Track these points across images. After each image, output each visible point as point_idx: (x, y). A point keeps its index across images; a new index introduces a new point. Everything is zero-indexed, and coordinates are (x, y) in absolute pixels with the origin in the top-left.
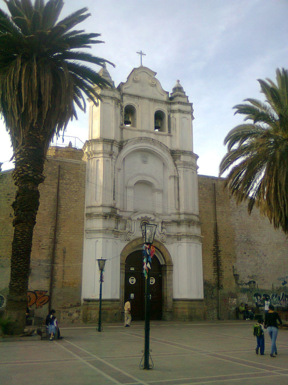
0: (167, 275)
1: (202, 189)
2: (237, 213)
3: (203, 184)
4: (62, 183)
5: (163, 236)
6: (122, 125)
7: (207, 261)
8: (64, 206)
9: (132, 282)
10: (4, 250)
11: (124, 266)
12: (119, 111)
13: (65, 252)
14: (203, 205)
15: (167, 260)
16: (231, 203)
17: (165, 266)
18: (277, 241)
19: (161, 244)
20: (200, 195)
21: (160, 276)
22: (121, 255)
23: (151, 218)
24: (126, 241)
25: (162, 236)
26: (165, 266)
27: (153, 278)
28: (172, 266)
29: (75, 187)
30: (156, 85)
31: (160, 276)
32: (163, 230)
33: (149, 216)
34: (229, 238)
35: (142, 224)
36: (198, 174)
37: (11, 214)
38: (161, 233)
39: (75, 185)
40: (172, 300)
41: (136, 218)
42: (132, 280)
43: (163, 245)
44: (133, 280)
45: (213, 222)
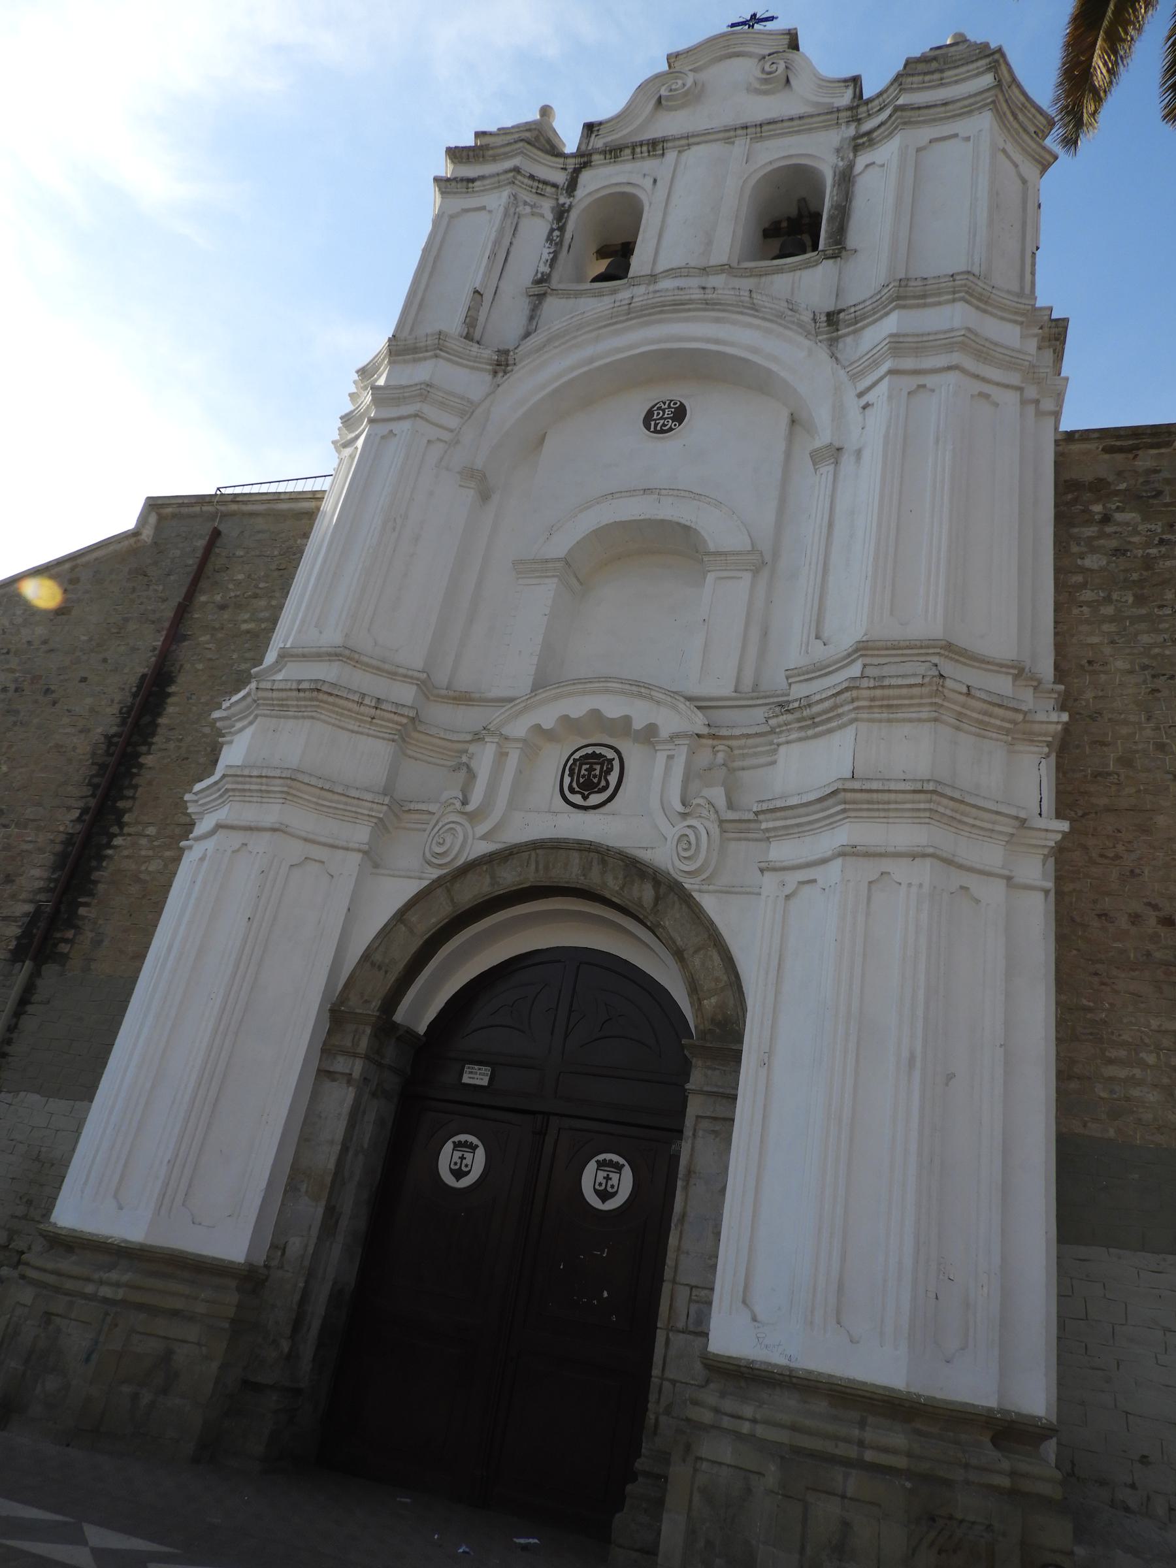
3: (1123, 486)
4: (206, 603)
5: (689, 832)
7: (1151, 1059)
8: (177, 709)
9: (458, 1174)
11: (368, 1031)
12: (536, 230)
13: (102, 941)
14: (1112, 619)
20: (1092, 562)
22: (366, 957)
23: (627, 720)
27: (622, 1161)
29: (262, 615)
30: (788, 81)
33: (613, 708)
36: (1066, 425)
39: (263, 603)
41: (519, 728)
42: (462, 1158)
44: (469, 1156)
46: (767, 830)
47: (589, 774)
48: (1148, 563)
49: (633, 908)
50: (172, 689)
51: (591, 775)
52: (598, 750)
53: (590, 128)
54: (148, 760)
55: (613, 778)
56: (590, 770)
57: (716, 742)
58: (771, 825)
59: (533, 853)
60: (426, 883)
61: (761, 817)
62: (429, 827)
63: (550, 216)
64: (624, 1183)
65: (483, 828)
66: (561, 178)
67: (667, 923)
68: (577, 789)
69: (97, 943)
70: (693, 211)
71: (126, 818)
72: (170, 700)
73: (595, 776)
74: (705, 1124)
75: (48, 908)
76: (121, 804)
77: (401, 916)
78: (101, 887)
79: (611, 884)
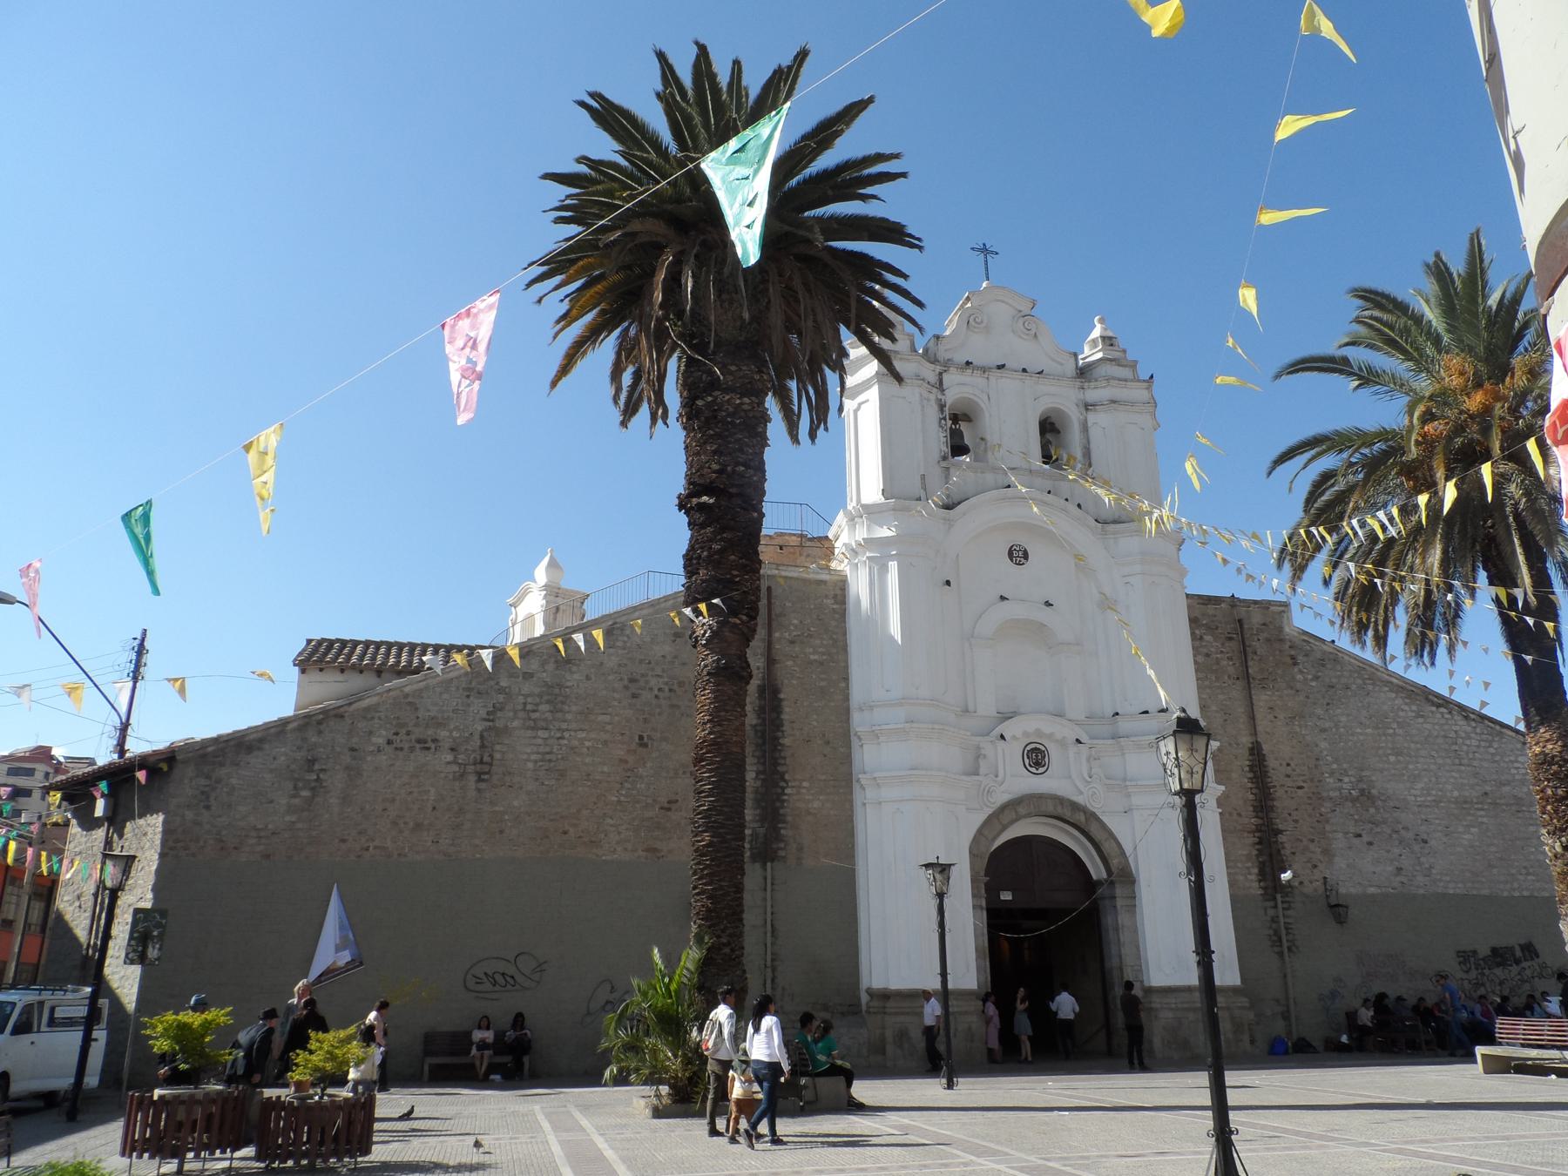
1: (1201, 638)
2: (1319, 711)
6: (944, 458)
10: (629, 846)
15: (1114, 862)
16: (1299, 677)
18: (1456, 794)
26: (1112, 883)
33: (1047, 729)
34: (1300, 788)
37: (641, 738)
45: (1246, 740)
48: (1218, 662)
50: (782, 696)
51: (1036, 758)
53: (937, 337)
54: (786, 741)
63: (936, 408)
66: (933, 378)
69: (800, 849)
70: (1009, 424)
71: (787, 777)
72: (784, 703)
75: (762, 831)
76: (780, 769)
77: (980, 832)
78: (789, 818)
79: (1067, 814)
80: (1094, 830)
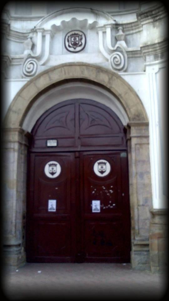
0: (133, 150)
9: (53, 174)
11: (17, 133)
15: (133, 110)
17: (129, 126)
19: (113, 74)
21: (123, 155)
24: (23, 77)
25: (115, 56)
28: (147, 125)
31: (123, 155)
32: (118, 43)
35: (67, 37)
38: (112, 49)
40: (149, 215)
42: (53, 169)
43: (119, 77)
44: (55, 168)
46: (145, 53)
47: (75, 41)
49: (102, 83)
52: (76, 32)
55: (83, 41)
56: (75, 39)
57: (117, 26)
58: (146, 51)
59: (63, 69)
60: (25, 83)
61: (142, 49)
62: (22, 63)
64: (108, 168)
65: (42, 62)
67: (114, 86)
68: (71, 46)
73: (77, 41)
74: (138, 146)
79: (92, 76)
80: (116, 87)
